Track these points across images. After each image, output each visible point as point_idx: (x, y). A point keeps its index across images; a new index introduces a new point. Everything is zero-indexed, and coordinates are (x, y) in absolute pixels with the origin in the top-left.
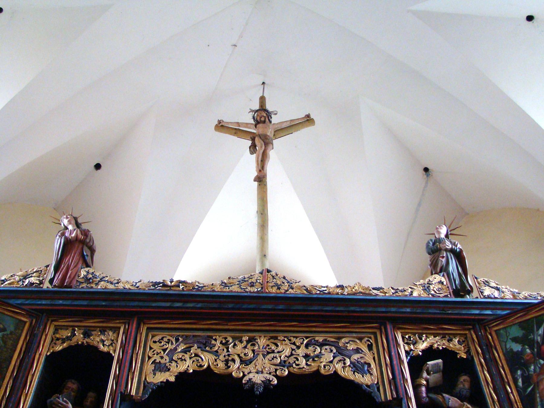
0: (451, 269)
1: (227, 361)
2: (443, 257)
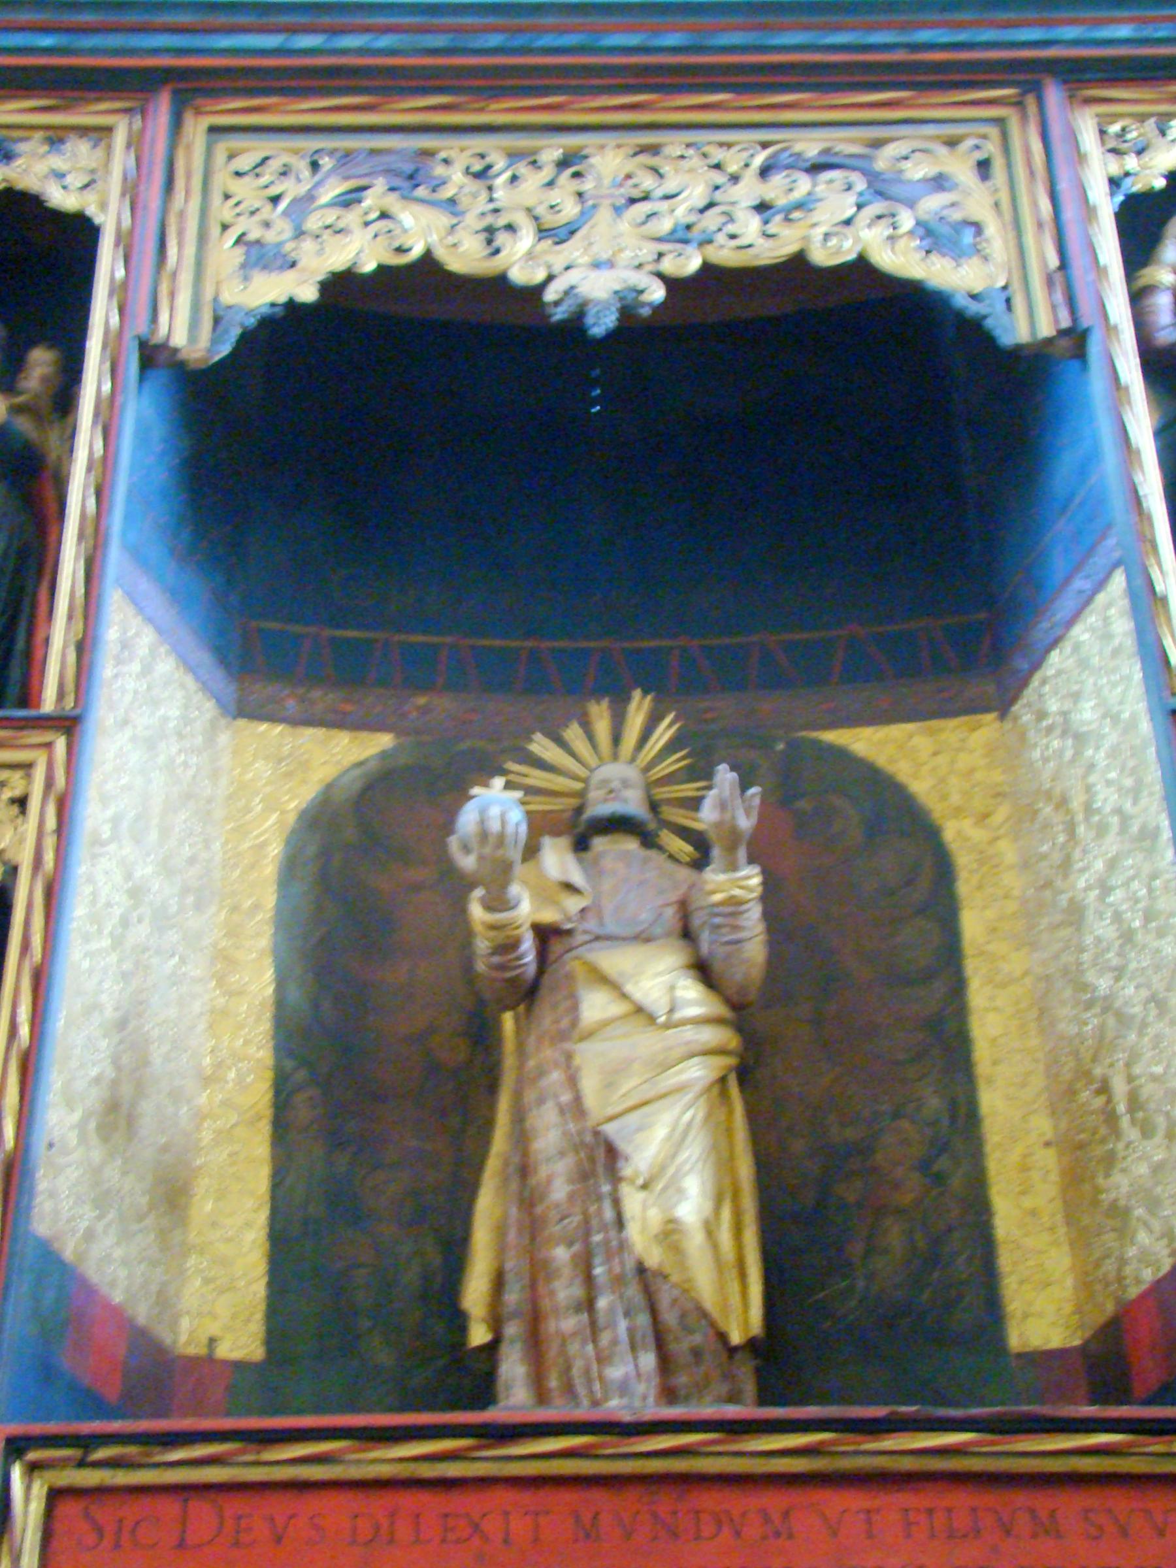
1: (490, 231)
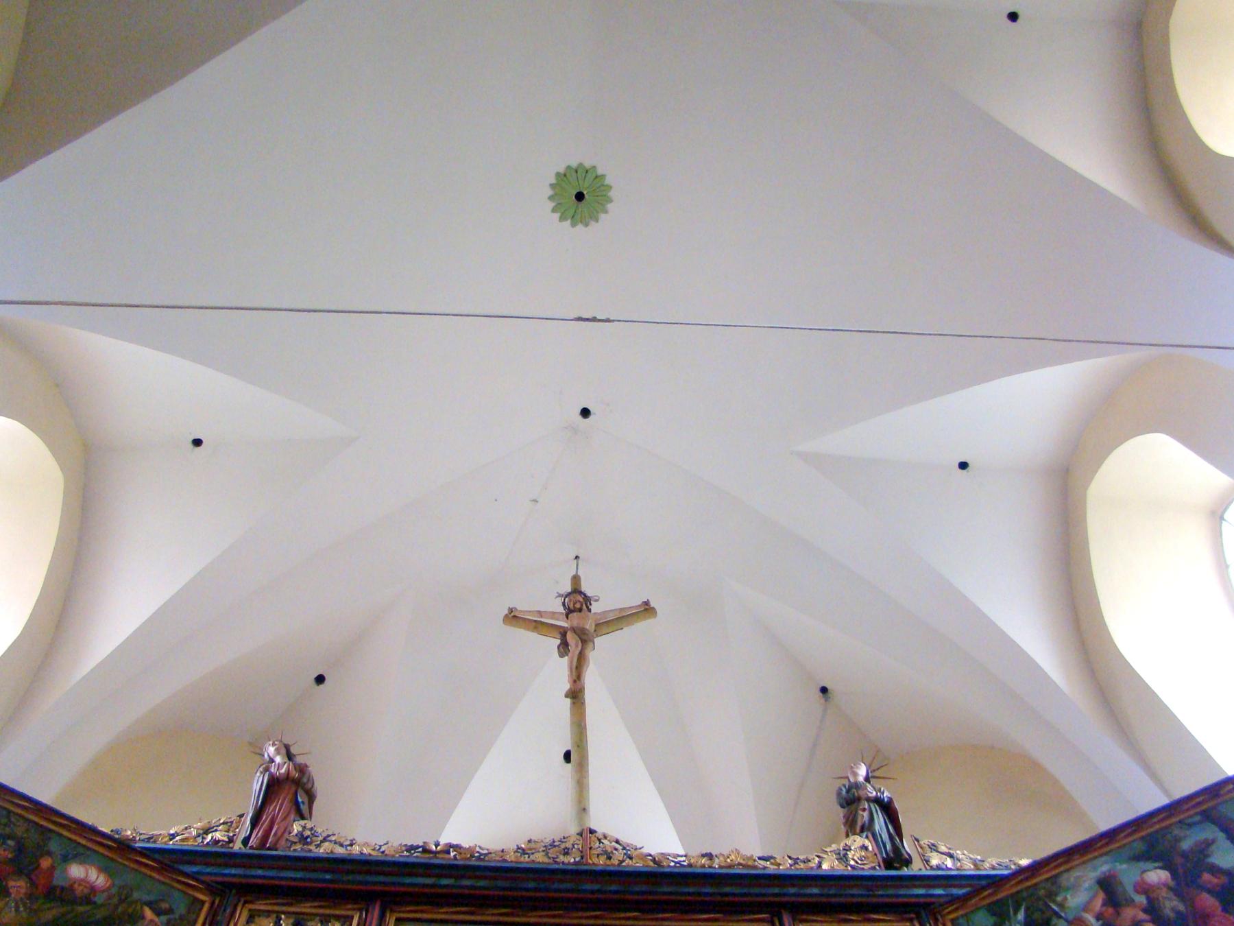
0: (877, 828)
2: (864, 810)
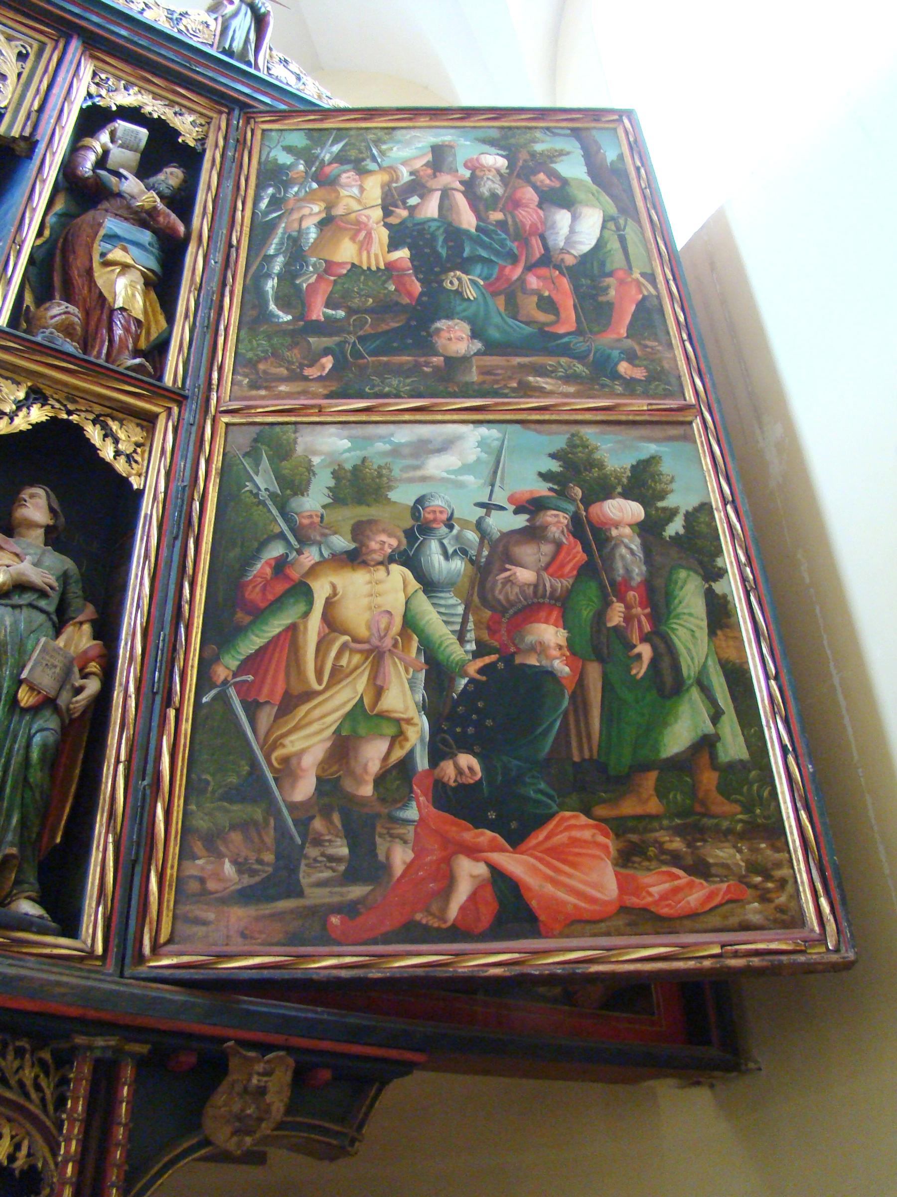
0: (235, 23)
